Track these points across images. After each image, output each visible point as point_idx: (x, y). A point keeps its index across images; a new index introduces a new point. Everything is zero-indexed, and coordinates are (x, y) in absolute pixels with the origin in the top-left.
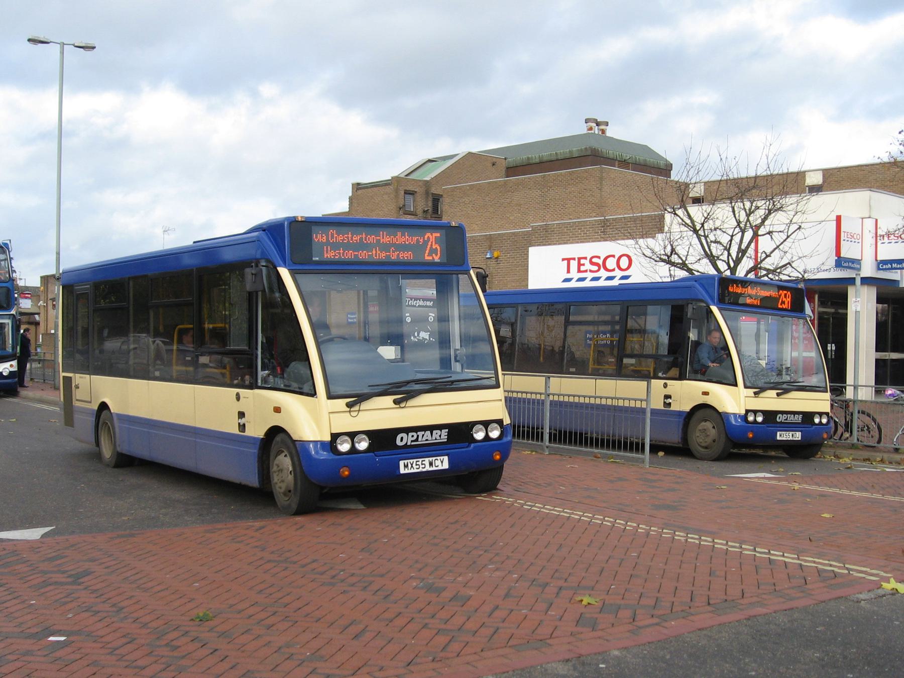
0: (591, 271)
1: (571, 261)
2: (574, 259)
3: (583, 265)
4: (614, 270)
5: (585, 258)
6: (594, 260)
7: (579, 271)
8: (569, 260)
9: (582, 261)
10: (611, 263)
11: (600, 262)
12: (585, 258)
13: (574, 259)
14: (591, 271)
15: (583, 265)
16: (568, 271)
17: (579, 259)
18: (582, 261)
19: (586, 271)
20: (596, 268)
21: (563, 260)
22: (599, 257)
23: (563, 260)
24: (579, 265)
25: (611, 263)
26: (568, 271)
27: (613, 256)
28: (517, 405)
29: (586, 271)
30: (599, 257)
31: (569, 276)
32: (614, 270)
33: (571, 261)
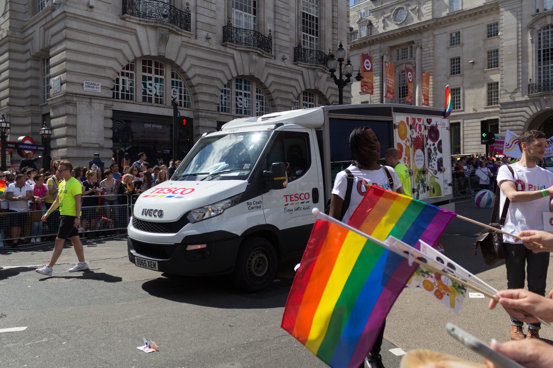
0: (295, 200)
1: (287, 197)
2: (288, 196)
3: (292, 198)
4: (303, 199)
5: (293, 195)
6: (296, 196)
7: (291, 201)
8: (286, 196)
9: (292, 196)
10: (302, 197)
11: (298, 196)
12: (293, 195)
13: (288, 196)
14: (295, 200)
15: (292, 198)
16: (287, 201)
17: (291, 195)
18: (292, 196)
19: (293, 200)
20: (297, 199)
21: (284, 196)
22: (298, 194)
23: (284, 196)
24: (291, 198)
25: (302, 197)
26: (287, 201)
27: (303, 194)
28: (493, 101)
29: (293, 200)
30: (298, 194)
31: (287, 203)
32: (303, 199)
33: (287, 197)
